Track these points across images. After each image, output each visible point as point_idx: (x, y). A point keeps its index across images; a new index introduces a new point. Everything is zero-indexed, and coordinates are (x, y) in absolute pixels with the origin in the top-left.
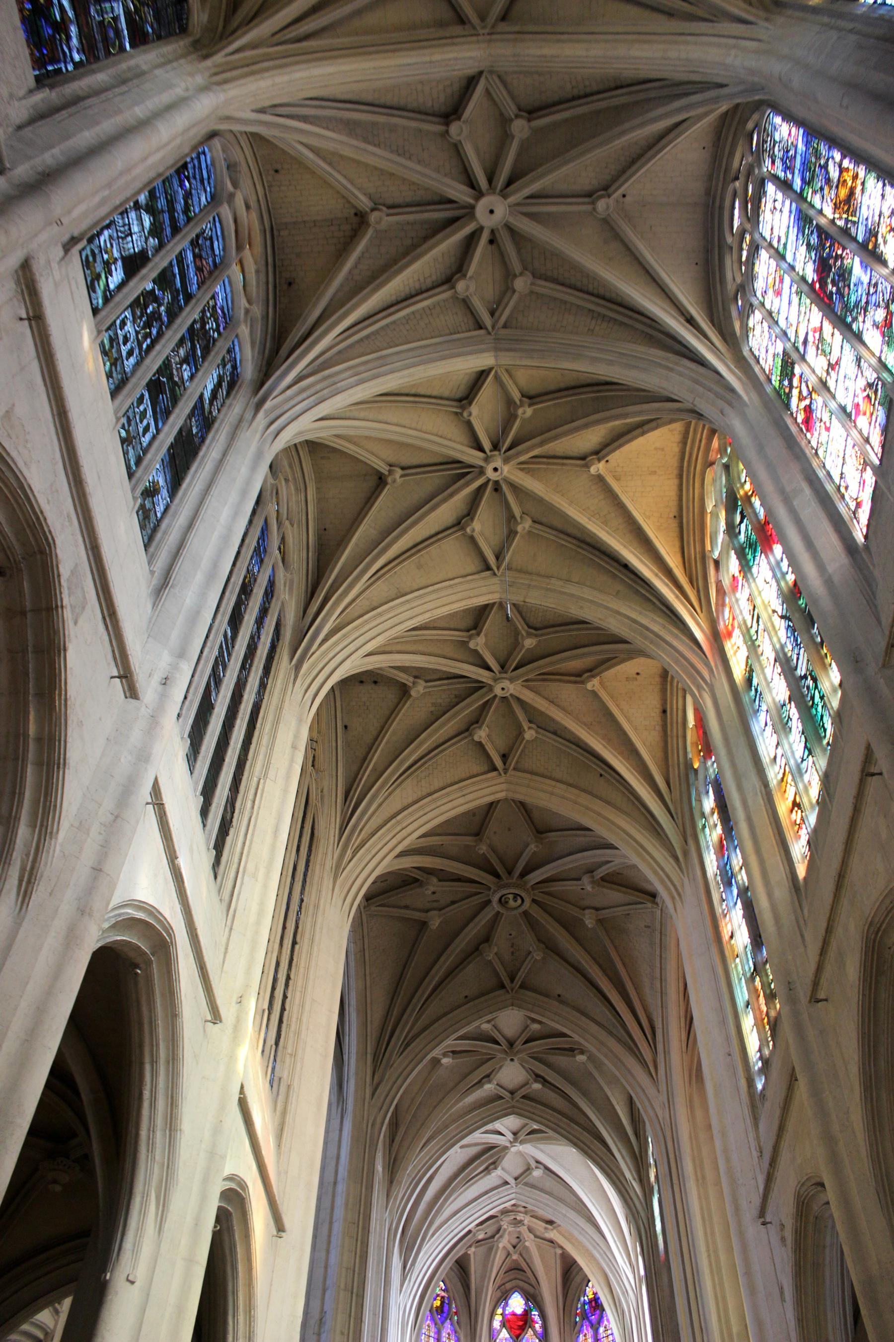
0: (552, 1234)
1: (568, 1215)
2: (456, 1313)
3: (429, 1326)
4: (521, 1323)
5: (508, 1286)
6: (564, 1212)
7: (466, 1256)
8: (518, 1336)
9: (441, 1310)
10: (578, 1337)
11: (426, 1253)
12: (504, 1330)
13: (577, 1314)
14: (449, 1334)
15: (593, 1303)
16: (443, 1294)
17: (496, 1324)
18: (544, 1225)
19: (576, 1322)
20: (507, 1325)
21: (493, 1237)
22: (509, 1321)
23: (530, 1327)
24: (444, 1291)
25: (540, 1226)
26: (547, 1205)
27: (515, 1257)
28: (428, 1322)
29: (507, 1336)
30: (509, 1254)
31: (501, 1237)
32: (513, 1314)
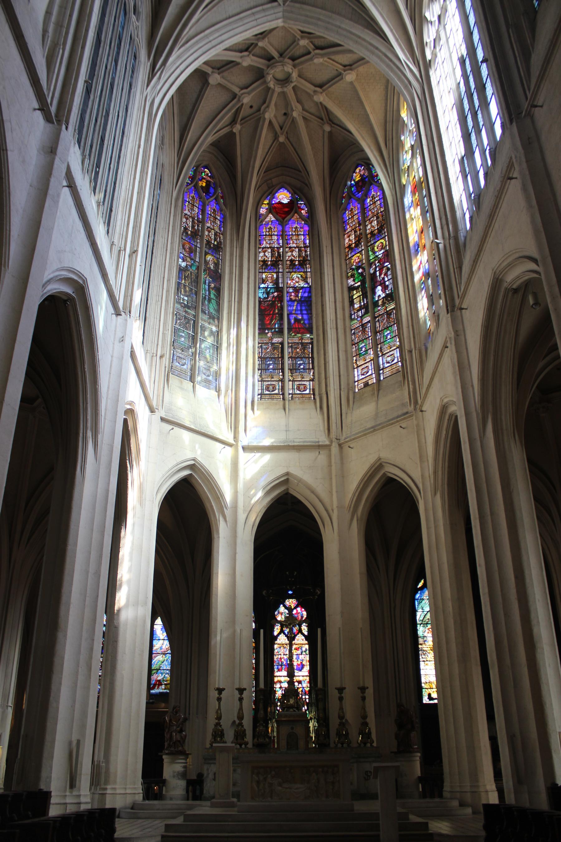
0: (321, 98)
1: (343, 26)
2: (222, 197)
3: (193, 197)
4: (286, 210)
5: (275, 181)
6: (338, 23)
7: (231, 136)
8: (284, 219)
9: (206, 190)
10: (345, 213)
11: (179, 57)
12: (271, 215)
13: (344, 197)
14: (214, 210)
15: (360, 184)
16: (209, 179)
17: (263, 211)
18: (312, 87)
19: (342, 203)
20: (273, 211)
21: (259, 110)
22: (275, 208)
23: (296, 212)
24: (210, 177)
25: (309, 88)
26: (319, 19)
27: (282, 139)
28: (193, 195)
29: (273, 219)
30: (276, 137)
31: (268, 107)
32: (280, 203)
